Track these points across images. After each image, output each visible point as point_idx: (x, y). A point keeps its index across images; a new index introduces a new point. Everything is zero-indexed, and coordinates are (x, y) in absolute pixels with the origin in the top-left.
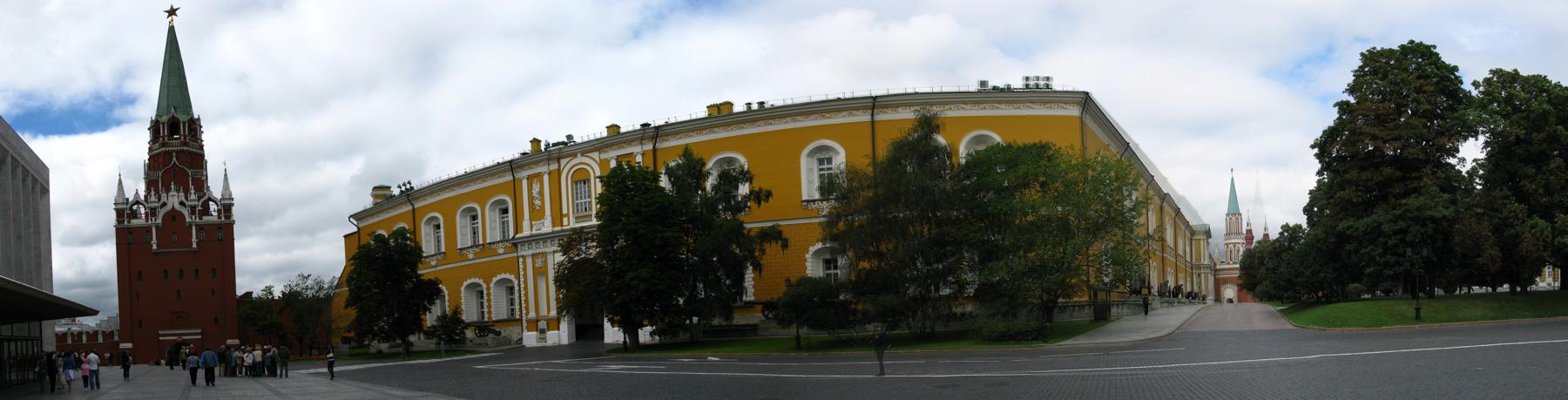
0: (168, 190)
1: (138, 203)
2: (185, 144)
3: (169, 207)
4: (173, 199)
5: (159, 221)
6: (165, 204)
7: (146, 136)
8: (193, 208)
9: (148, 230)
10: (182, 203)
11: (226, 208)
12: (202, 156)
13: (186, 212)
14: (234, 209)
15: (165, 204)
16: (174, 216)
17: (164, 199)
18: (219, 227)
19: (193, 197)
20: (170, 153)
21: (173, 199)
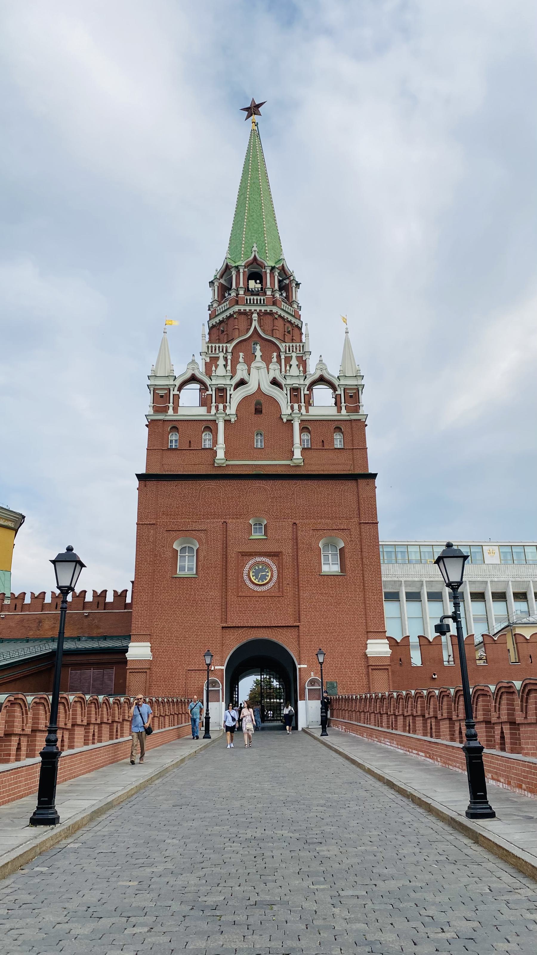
0: (250, 359)
1: (193, 379)
2: (274, 303)
3: (251, 388)
4: (259, 376)
5: (232, 409)
6: (242, 382)
7: (208, 295)
8: (295, 391)
9: (210, 426)
10: (275, 382)
11: (351, 397)
12: (300, 329)
13: (282, 397)
14: (363, 398)
15: (242, 382)
16: (258, 405)
17: (241, 372)
18: (338, 426)
19: (294, 371)
20: (248, 315)
21: (259, 376)
